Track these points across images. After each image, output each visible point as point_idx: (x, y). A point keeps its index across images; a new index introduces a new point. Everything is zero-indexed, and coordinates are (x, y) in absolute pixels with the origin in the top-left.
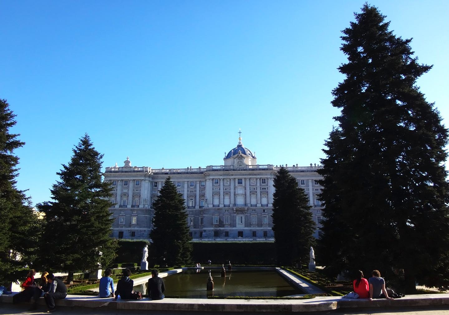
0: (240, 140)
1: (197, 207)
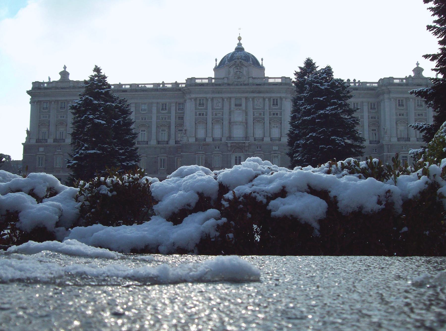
0: (240, 39)
1: (172, 143)
